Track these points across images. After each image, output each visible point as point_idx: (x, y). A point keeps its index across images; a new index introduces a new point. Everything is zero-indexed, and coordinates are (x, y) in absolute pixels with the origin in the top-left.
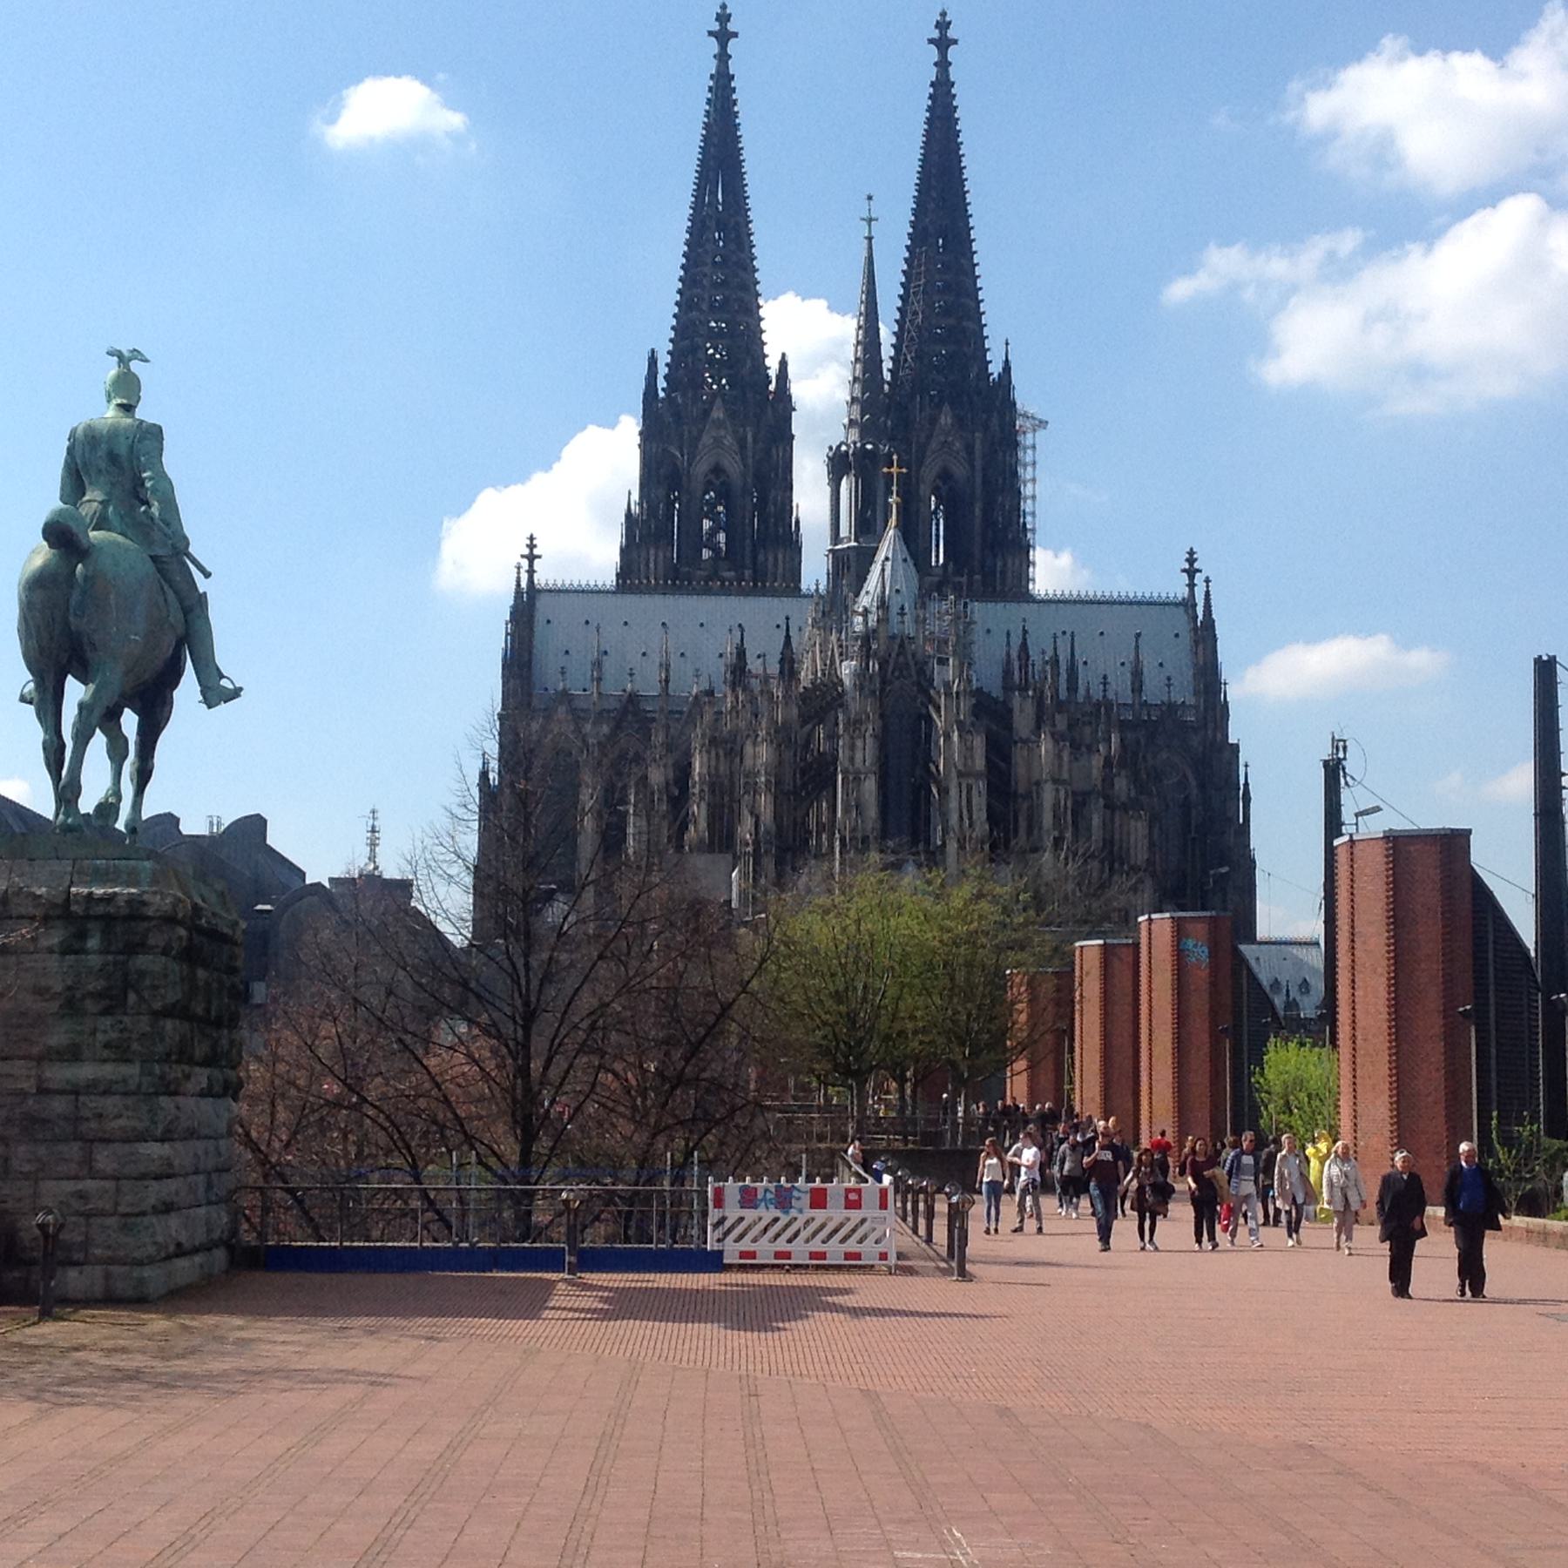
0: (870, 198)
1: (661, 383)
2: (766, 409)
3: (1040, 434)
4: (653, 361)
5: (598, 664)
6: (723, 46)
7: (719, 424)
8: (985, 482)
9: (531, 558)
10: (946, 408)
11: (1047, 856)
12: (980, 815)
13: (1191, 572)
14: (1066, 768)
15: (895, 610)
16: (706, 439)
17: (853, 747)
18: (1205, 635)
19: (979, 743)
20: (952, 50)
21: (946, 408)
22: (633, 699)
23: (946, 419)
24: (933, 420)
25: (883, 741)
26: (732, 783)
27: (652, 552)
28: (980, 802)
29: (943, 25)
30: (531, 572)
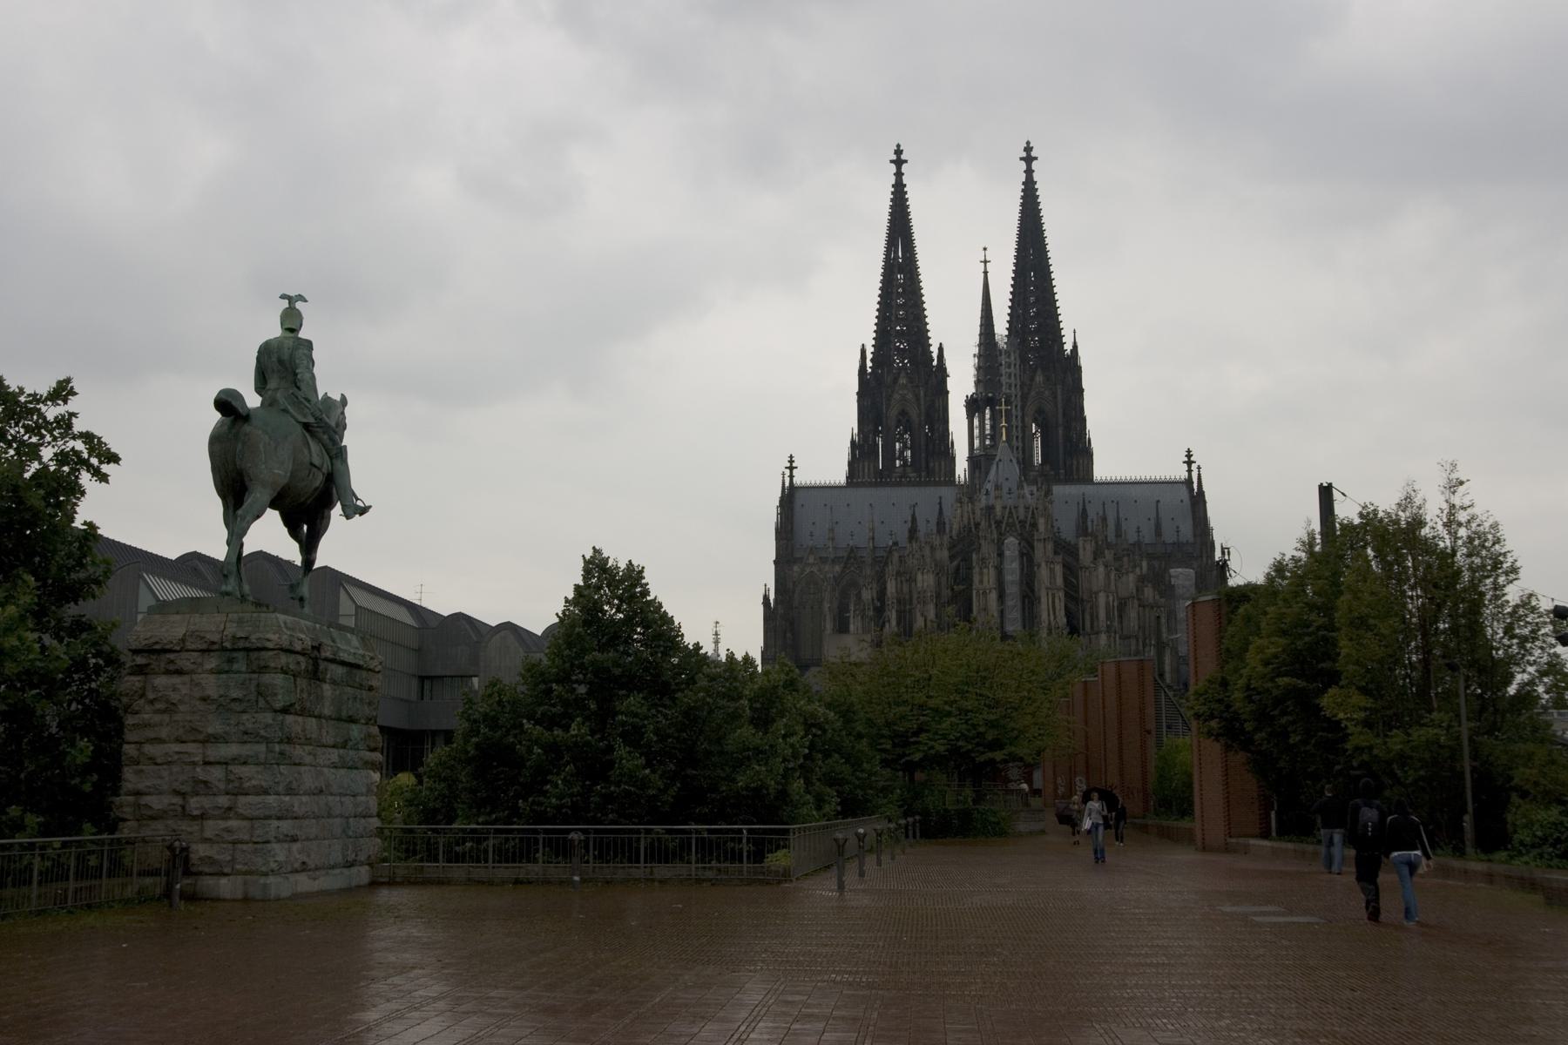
4: (863, 352)
9: (791, 468)
10: (1039, 372)
12: (1061, 614)
16: (896, 396)
19: (1059, 569)
21: (1039, 372)
23: (1039, 378)
28: (1060, 606)
30: (791, 477)
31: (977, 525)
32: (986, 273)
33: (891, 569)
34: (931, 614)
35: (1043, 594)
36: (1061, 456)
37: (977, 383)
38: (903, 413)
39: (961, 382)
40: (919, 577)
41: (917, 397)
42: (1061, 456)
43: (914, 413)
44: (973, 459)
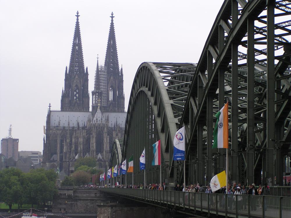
0: (98, 55)
2: (85, 76)
4: (67, 68)
5: (59, 123)
6: (78, 18)
8: (118, 87)
15: (98, 120)
16: (75, 81)
17: (92, 139)
19: (108, 139)
20: (114, 18)
21: (112, 76)
22: (64, 127)
26: (78, 142)
29: (112, 14)
30: (50, 108)
31: (92, 128)
32: (98, 61)
33: (74, 136)
34: (82, 147)
35: (105, 144)
37: (95, 88)
38: (77, 86)
39: (91, 87)
43: (79, 85)
44: (93, 107)
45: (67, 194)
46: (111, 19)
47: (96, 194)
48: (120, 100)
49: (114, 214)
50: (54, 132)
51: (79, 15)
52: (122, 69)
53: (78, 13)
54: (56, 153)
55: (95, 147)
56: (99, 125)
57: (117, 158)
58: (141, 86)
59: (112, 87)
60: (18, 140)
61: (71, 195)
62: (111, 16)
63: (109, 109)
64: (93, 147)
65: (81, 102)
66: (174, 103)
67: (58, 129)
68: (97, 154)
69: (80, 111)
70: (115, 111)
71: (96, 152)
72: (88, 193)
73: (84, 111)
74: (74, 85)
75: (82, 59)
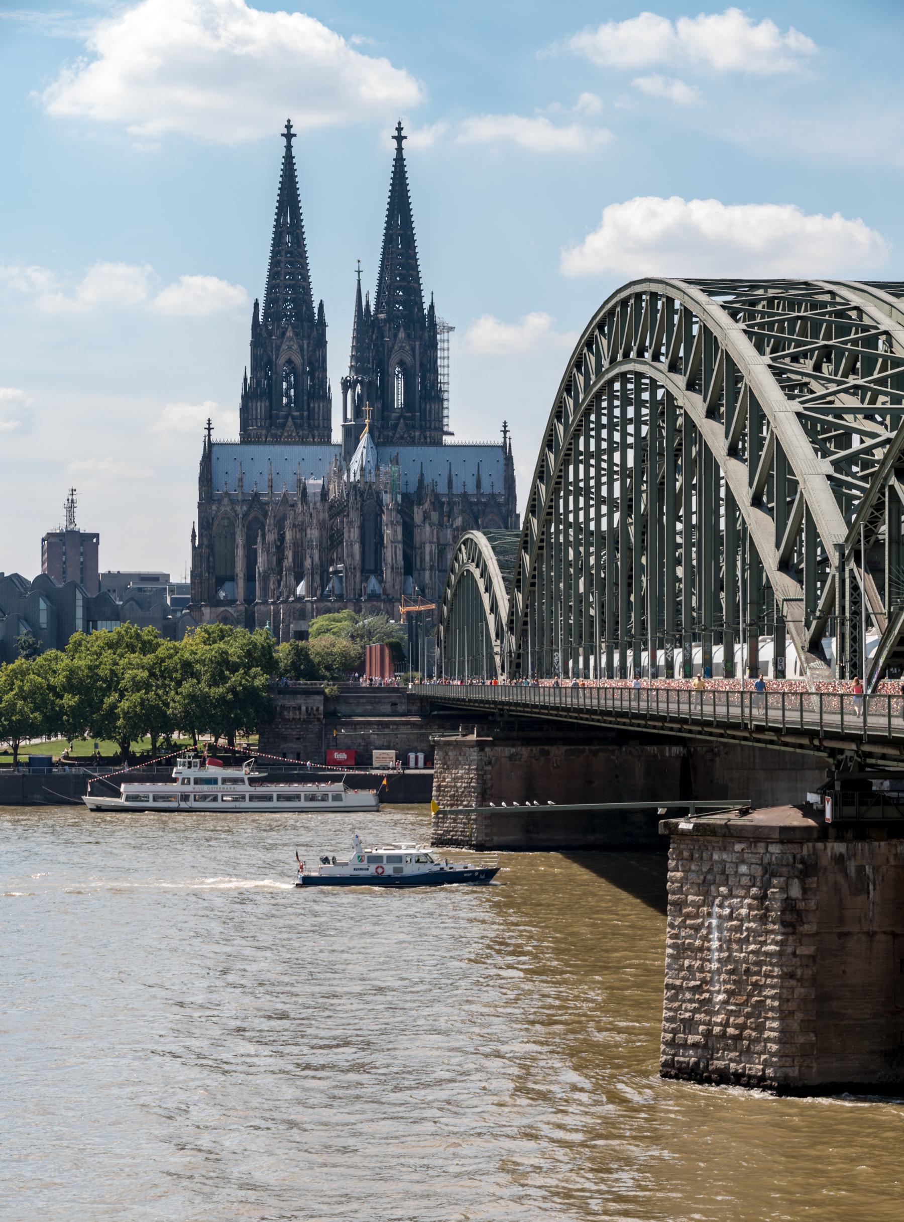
1: (261, 318)
2: (313, 330)
3: (451, 333)
4: (256, 305)
5: (241, 480)
6: (289, 142)
7: (291, 339)
8: (421, 364)
10: (402, 329)
11: (427, 573)
12: (400, 558)
13: (505, 432)
14: (435, 536)
15: (367, 471)
16: (284, 347)
17: (350, 532)
18: (509, 460)
19: (399, 529)
21: (402, 329)
22: (257, 495)
23: (401, 335)
24: (395, 336)
25: (362, 528)
26: (302, 542)
27: (259, 404)
28: (400, 553)
32: (359, 281)
36: (417, 401)
37: (351, 367)
38: (289, 362)
40: (309, 532)
41: (301, 348)
42: (417, 401)
43: (297, 360)
45: (304, 708)
46: (395, 143)
47: (394, 704)
48: (428, 406)
49: (489, 768)
50: (223, 509)
51: (293, 131)
52: (432, 307)
53: (289, 127)
54: (232, 578)
55: (358, 557)
56: (370, 486)
57: (482, 588)
58: (620, 358)
59: (401, 363)
60: (97, 536)
61: (318, 710)
62: (396, 134)
63: (394, 434)
64: (352, 556)
65: (305, 413)
66: (805, 409)
67: (233, 502)
68: (366, 579)
69: (303, 442)
70: (412, 443)
71: (363, 570)
72: (371, 704)
73: (314, 443)
74: (282, 360)
75: (306, 278)
